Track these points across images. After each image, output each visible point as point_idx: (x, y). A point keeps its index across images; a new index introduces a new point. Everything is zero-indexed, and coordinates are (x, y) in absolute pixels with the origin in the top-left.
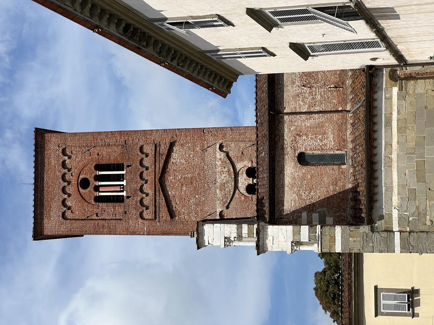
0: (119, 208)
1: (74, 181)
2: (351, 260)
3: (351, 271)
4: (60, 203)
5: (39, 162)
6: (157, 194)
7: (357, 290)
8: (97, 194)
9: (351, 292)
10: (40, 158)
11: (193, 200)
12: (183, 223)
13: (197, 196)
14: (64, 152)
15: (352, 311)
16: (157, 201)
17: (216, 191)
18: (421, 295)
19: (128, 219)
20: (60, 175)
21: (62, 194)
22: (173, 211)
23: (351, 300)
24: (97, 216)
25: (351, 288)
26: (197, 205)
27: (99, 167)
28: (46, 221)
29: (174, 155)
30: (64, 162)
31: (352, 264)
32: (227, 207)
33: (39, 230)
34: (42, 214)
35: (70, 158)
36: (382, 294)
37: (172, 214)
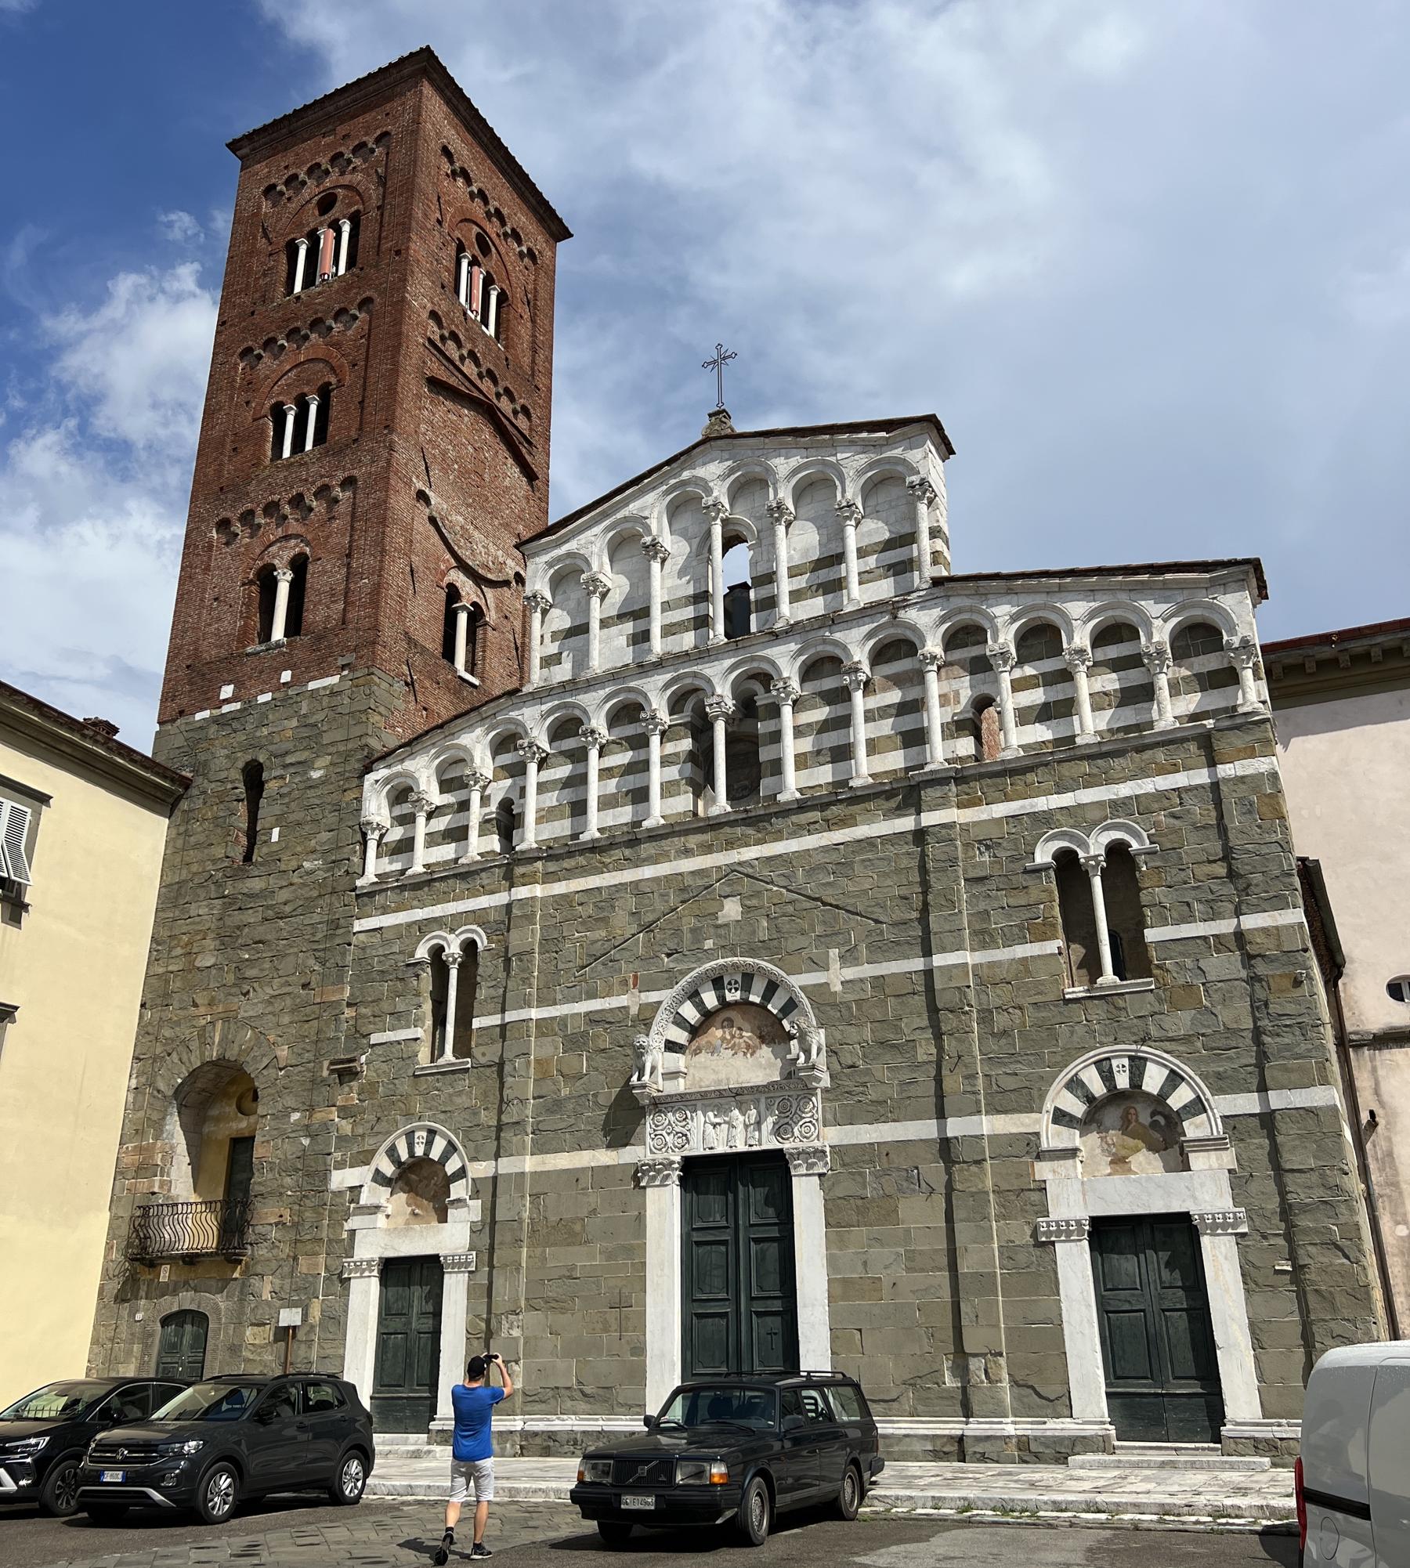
0: (447, 277)
1: (492, 228)
2: (133, 761)
3: (109, 749)
4: (466, 166)
5: (527, 194)
6: (467, 384)
7: (52, 743)
8: (468, 254)
9: (61, 725)
10: (531, 199)
11: (452, 454)
12: (419, 397)
13: (456, 466)
14: (531, 254)
15: (14, 702)
16: (457, 373)
17: (461, 514)
18: (5, 929)
19: (433, 282)
20: (505, 211)
21: (481, 185)
22: (438, 393)
23: (42, 715)
24: (438, 221)
25: (70, 728)
26: (444, 453)
27: (502, 298)
28: (445, 108)
29: (516, 471)
30: (520, 242)
31: (124, 759)
32: (432, 520)
33: (435, 75)
34: (455, 110)
35: (521, 255)
36: (29, 811)
37: (435, 384)
